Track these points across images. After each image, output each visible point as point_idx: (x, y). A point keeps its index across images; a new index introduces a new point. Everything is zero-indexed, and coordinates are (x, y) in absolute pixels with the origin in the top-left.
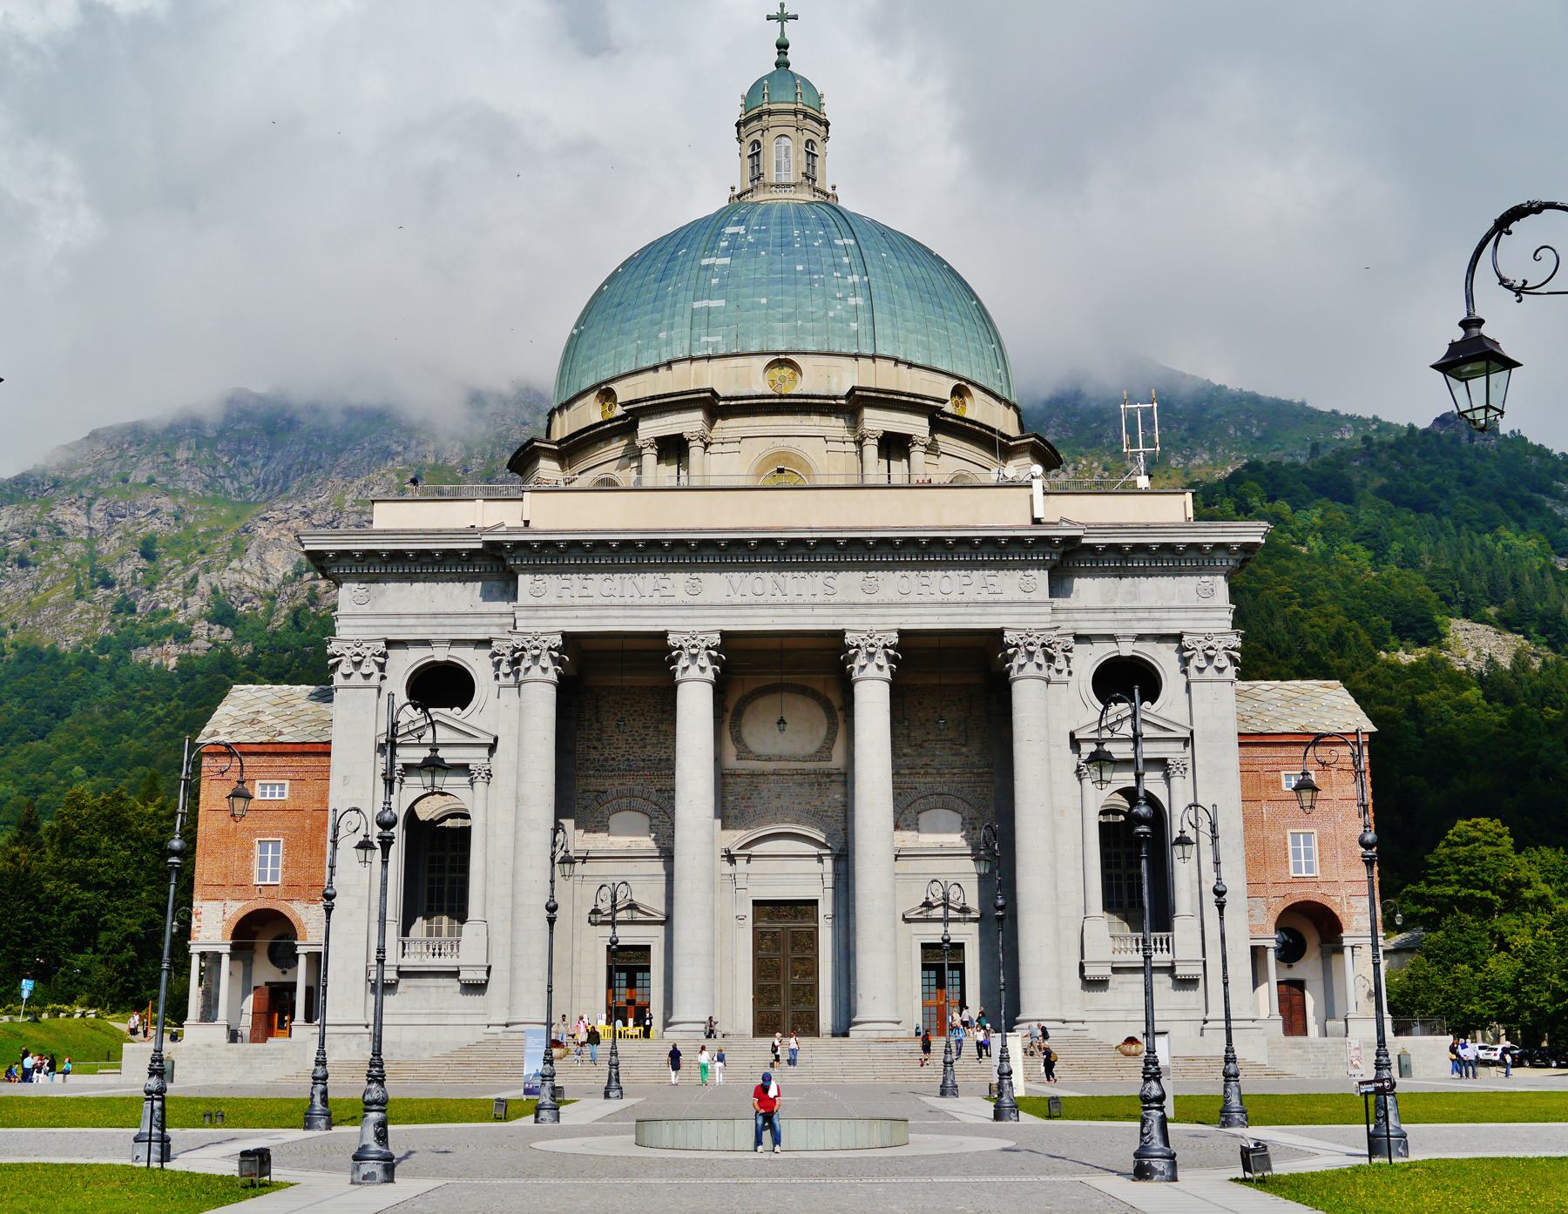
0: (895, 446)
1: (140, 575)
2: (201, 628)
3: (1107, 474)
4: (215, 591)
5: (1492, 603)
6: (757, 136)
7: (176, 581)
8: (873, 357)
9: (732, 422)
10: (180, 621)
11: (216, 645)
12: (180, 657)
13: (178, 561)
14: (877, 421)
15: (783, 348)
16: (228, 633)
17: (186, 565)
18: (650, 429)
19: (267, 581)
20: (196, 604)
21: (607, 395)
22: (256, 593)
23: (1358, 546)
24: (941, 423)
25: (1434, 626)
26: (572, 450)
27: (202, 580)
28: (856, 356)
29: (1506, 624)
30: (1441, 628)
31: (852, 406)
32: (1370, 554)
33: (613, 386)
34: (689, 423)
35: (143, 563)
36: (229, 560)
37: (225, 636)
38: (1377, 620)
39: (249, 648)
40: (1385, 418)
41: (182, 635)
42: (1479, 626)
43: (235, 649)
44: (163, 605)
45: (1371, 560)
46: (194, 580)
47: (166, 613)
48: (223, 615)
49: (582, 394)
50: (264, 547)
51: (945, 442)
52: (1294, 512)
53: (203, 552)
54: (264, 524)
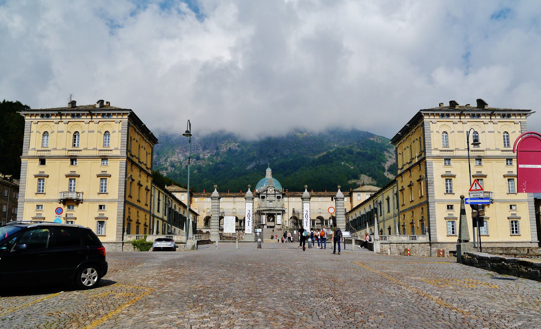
1: (157, 158)
2: (169, 168)
3: (320, 142)
4: (171, 161)
5: (368, 172)
7: (163, 159)
10: (165, 166)
11: (172, 171)
12: (166, 173)
13: (163, 155)
16: (173, 169)
17: (165, 156)
19: (179, 159)
20: (168, 164)
22: (177, 161)
23: (351, 162)
25: (358, 177)
27: (169, 160)
29: (369, 176)
30: (359, 177)
32: (353, 164)
35: (157, 156)
36: (172, 155)
37: (173, 169)
38: (350, 176)
39: (178, 173)
40: (369, 132)
41: (166, 169)
42: (366, 176)
43: (176, 171)
44: (161, 163)
45: (353, 164)
46: (167, 159)
47: (163, 165)
48: (173, 166)
50: (178, 153)
52: (343, 156)
53: (167, 154)
54: (178, 149)
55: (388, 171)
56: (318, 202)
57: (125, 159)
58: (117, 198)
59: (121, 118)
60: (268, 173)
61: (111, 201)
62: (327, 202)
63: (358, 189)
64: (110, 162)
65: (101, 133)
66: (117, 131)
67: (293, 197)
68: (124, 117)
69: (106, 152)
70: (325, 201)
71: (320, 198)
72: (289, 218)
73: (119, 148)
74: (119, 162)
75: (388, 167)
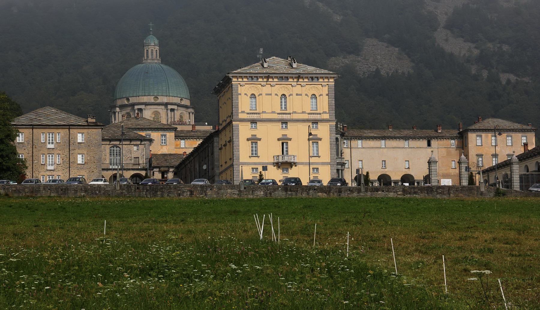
0: (172, 110)
6: (148, 49)
8: (169, 96)
9: (148, 106)
14: (170, 107)
15: (156, 94)
18: (136, 107)
21: (128, 100)
24: (179, 105)
26: (122, 107)
28: (167, 96)
31: (166, 105)
33: (129, 98)
34: (142, 107)
42: (380, 43)
49: (124, 98)
51: (179, 108)
55: (450, 26)
56: (403, 148)
57: (335, 123)
58: (330, 161)
59: (328, 82)
60: (150, 51)
61: (323, 164)
62: (420, 148)
63: (476, 126)
64: (320, 125)
65: (308, 96)
66: (324, 95)
67: (359, 139)
68: (331, 80)
69: (315, 115)
70: (415, 146)
71: (407, 142)
72: (353, 178)
73: (328, 112)
74: (329, 125)
75: (446, 14)
